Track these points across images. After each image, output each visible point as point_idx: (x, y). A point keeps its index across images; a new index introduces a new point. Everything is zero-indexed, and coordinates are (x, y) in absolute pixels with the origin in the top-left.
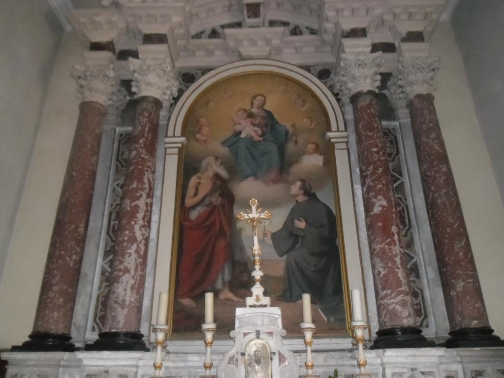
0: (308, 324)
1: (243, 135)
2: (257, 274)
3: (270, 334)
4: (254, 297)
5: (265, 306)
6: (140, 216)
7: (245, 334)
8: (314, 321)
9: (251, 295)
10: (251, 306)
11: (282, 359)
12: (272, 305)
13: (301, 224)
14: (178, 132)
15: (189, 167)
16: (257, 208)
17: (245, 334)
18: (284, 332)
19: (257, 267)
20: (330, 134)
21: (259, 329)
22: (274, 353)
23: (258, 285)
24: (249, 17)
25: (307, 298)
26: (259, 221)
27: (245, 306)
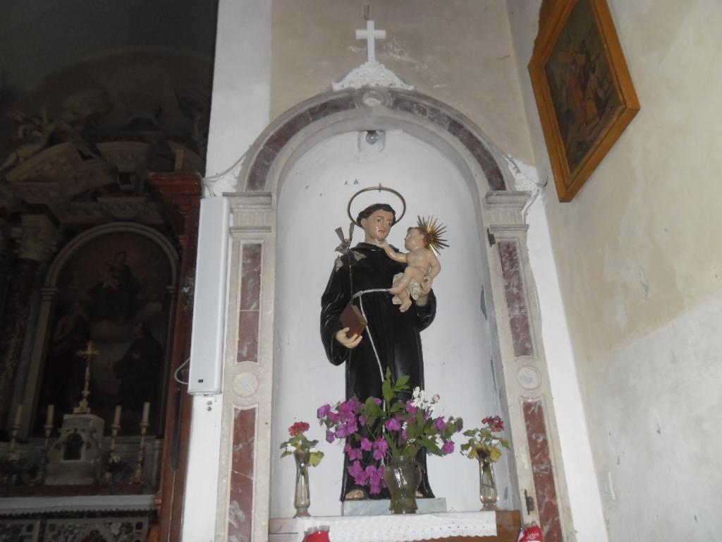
0: (116, 424)
1: (104, 286)
2: (86, 393)
3: (83, 431)
7: (68, 431)
10: (76, 414)
11: (89, 446)
12: (92, 413)
13: (137, 356)
14: (54, 280)
15: (59, 310)
17: (68, 431)
19: (86, 388)
20: (169, 287)
21: (76, 427)
22: (83, 442)
23: (85, 400)
25: (118, 409)
26: (100, 357)
27: (71, 412)
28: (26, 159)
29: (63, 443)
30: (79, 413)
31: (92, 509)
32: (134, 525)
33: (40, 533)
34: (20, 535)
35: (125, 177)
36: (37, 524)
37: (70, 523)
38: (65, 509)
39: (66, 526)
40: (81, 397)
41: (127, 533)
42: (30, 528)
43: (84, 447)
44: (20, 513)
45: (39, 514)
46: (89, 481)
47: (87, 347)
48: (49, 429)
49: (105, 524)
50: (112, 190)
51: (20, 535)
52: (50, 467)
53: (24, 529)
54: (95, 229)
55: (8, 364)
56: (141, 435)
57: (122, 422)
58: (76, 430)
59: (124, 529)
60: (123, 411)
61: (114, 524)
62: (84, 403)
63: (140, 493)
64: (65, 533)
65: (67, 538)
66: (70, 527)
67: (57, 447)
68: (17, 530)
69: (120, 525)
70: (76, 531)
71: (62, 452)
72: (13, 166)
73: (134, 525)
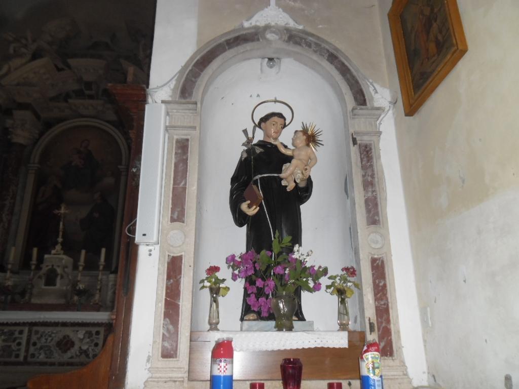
0: (82, 262)
1: (73, 164)
2: (60, 240)
3: (58, 266)
4: (56, 250)
7: (47, 266)
9: (55, 248)
11: (62, 277)
12: (64, 254)
13: (96, 215)
14: (37, 160)
15: (41, 181)
17: (47, 266)
20: (119, 167)
22: (58, 275)
23: (59, 245)
25: (83, 252)
27: (50, 253)
28: (16, 69)
29: (44, 274)
30: (55, 254)
31: (65, 321)
32: (94, 332)
33: (28, 336)
34: (14, 336)
35: (88, 85)
36: (26, 329)
37: (48, 330)
38: (45, 320)
39: (47, 332)
40: (56, 243)
41: (89, 338)
42: (21, 332)
43: (59, 278)
44: (14, 322)
45: (28, 323)
46: (62, 301)
47: (61, 208)
48: (34, 264)
49: (74, 331)
50: (79, 94)
51: (14, 336)
52: (35, 291)
54: (68, 122)
55: (5, 218)
56: (99, 271)
57: (85, 261)
58: (53, 266)
59: (87, 335)
60: (86, 253)
61: (80, 332)
62: (58, 247)
63: (98, 310)
64: (45, 336)
65: (46, 339)
66: (49, 332)
67: (40, 277)
68: (12, 333)
69: (84, 332)
70: (53, 335)
71: (43, 281)
72: (6, 74)
73: (94, 332)
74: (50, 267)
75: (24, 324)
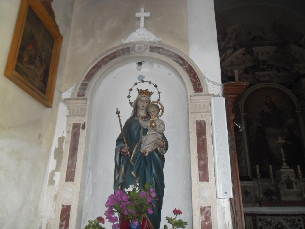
3: (292, 176)
5: (288, 169)
6: (243, 141)
7: (285, 177)
8: (301, 173)
11: (296, 183)
14: (243, 111)
16: (281, 139)
17: (285, 177)
18: (296, 176)
19: (283, 158)
20: (297, 111)
22: (293, 182)
24: (262, 65)
26: (277, 142)
27: (282, 169)
28: (228, 57)
29: (285, 182)
30: (284, 169)
34: (296, 223)
35: (264, 62)
40: (283, 162)
47: (279, 140)
48: (272, 175)
51: (296, 223)
52: (282, 192)
53: (296, 221)
58: (288, 176)
62: (285, 164)
67: (282, 183)
68: (294, 221)
71: (285, 186)
74: (287, 177)
75: (298, 215)
